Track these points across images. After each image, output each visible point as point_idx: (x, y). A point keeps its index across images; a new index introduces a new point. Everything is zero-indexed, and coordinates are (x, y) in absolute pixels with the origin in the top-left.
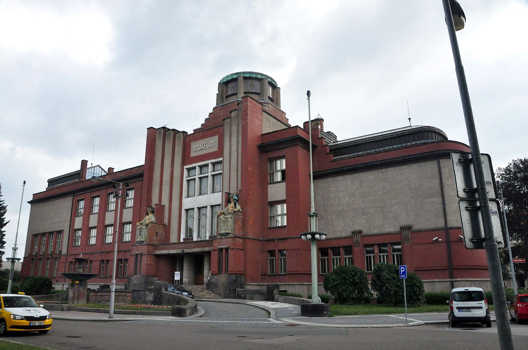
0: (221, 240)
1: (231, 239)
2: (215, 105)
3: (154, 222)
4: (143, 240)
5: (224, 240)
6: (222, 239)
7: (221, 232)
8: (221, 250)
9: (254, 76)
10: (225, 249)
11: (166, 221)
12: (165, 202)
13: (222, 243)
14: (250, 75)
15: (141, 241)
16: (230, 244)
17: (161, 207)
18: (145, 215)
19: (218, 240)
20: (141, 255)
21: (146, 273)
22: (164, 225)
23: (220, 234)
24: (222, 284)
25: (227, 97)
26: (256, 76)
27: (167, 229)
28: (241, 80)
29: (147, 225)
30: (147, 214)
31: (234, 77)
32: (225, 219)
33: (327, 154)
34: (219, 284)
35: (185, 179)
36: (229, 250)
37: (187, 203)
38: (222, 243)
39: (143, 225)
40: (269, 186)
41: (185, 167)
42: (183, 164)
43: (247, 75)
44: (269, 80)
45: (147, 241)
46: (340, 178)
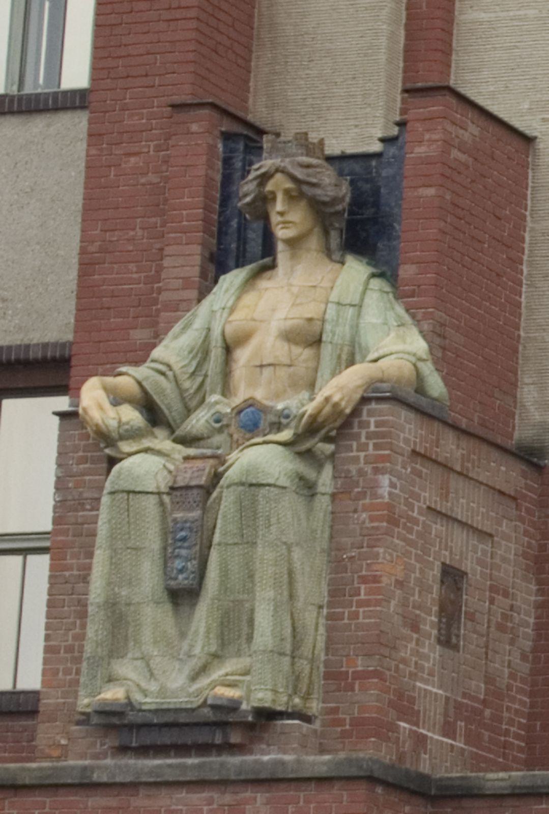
3: (420, 389)
4: (262, 697)
15: (232, 707)
39: (199, 421)
45: (315, 706)
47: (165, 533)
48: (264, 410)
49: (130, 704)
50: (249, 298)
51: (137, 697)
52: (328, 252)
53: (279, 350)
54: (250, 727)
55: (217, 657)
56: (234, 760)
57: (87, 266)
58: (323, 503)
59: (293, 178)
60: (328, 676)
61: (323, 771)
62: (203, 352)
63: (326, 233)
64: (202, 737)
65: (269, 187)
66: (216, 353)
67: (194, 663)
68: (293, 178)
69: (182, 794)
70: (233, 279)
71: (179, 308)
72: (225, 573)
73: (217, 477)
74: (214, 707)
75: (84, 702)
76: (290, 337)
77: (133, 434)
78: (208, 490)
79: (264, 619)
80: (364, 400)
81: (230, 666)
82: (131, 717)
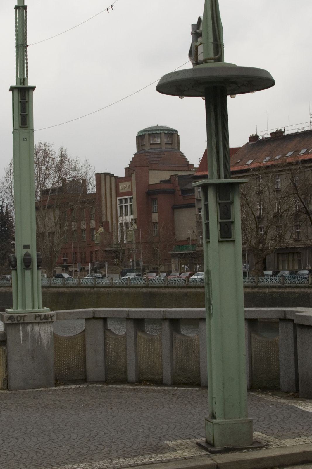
2: (135, 151)
9: (155, 132)
11: (110, 230)
12: (109, 220)
14: (152, 132)
17: (107, 222)
20: (98, 251)
22: (110, 233)
25: (142, 145)
26: (156, 132)
27: (111, 234)
28: (147, 136)
29: (99, 234)
30: (100, 227)
31: (144, 133)
33: (180, 195)
35: (118, 206)
37: (121, 220)
40: (152, 214)
41: (118, 198)
42: (116, 197)
43: (151, 133)
44: (166, 132)
46: (184, 209)
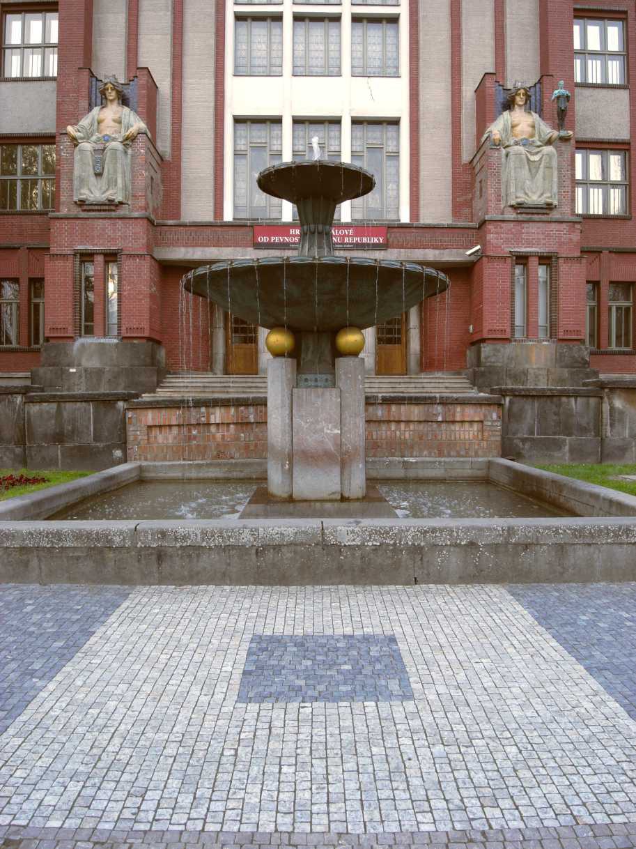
0: (523, 228)
1: (564, 225)
5: (533, 228)
6: (525, 225)
7: (522, 198)
8: (522, 259)
10: (537, 259)
13: (523, 236)
15: (113, 201)
16: (561, 244)
18: (84, 104)
19: (512, 225)
21: (151, 329)
23: (518, 207)
24: (544, 372)
32: (536, 158)
34: (531, 371)
36: (561, 261)
38: (523, 236)
45: (129, 203)
47: (93, 161)
48: (110, 137)
49: (87, 199)
50: (102, 112)
51: (89, 198)
52: (119, 103)
53: (112, 124)
54: (117, 206)
55: (107, 190)
56: (113, 213)
57: (59, 104)
58: (129, 156)
59: (113, 85)
60: (133, 196)
61: (136, 216)
62: (92, 125)
63: (119, 99)
64: (105, 208)
65: (107, 86)
66: (96, 124)
67: (102, 191)
68: (113, 85)
69: (101, 221)
70: (96, 110)
71: (83, 115)
72: (109, 170)
73: (105, 148)
74: (109, 200)
75: (75, 199)
76: (114, 121)
77: (81, 138)
78: (103, 150)
79: (120, 181)
80: (138, 134)
81: (110, 192)
82: (87, 203)
